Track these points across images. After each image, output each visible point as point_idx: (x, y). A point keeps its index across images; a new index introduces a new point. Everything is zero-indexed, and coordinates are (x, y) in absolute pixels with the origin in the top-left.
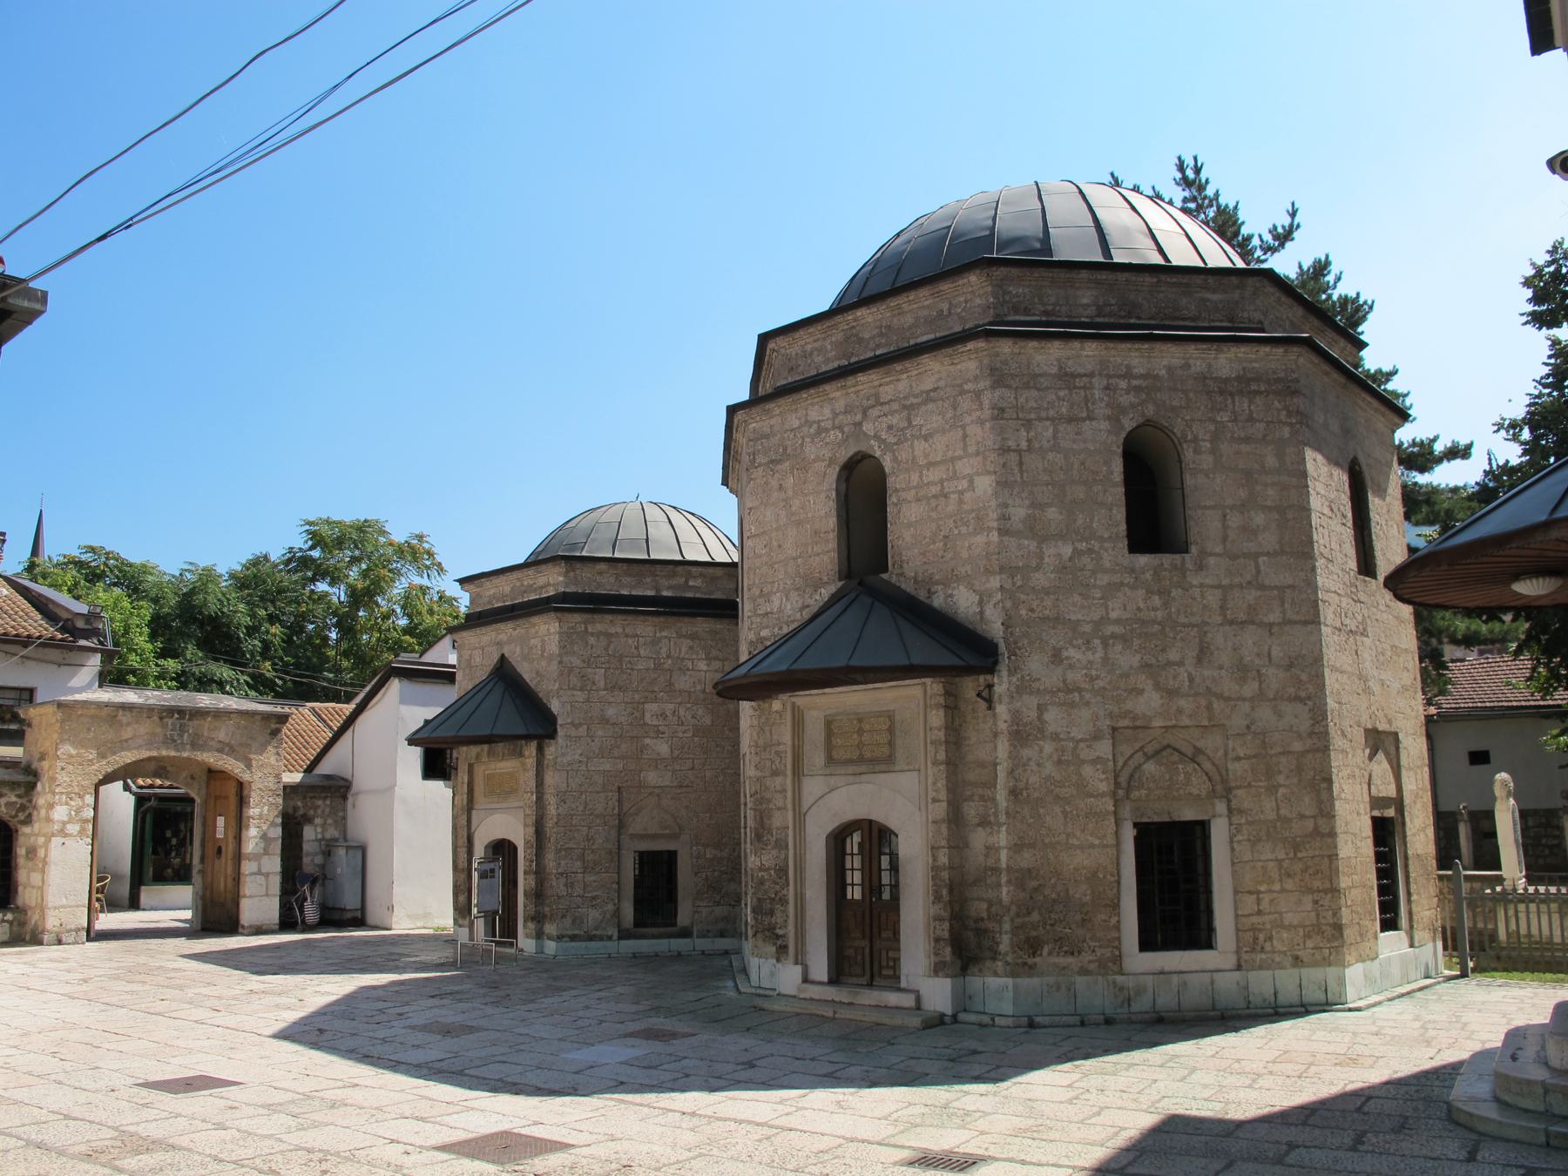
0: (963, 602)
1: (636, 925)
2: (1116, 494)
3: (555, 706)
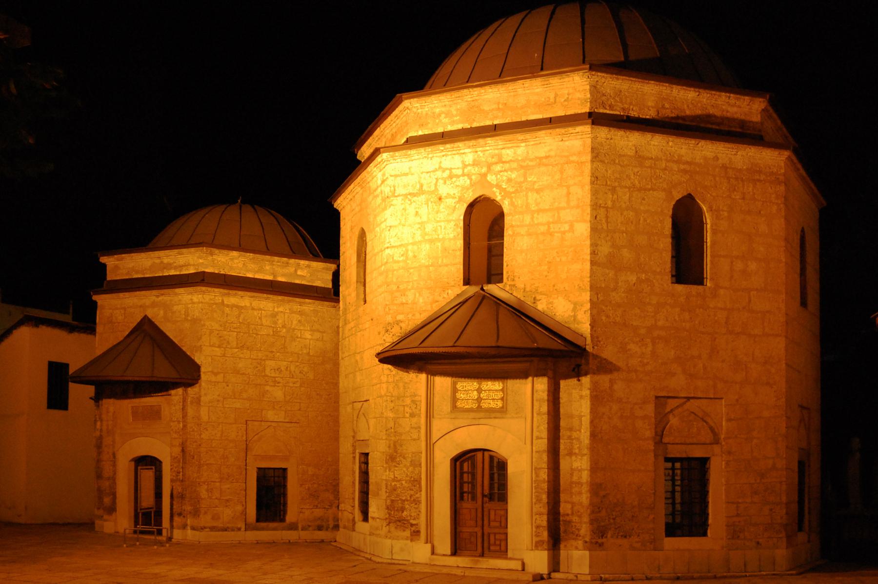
1: (258, 520)
3: (198, 359)
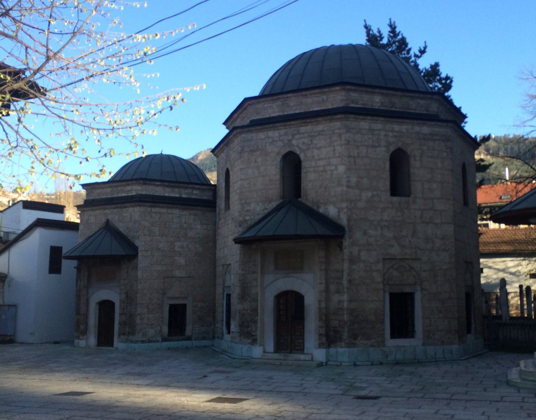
0: (332, 211)
2: (386, 175)
3: (137, 243)
